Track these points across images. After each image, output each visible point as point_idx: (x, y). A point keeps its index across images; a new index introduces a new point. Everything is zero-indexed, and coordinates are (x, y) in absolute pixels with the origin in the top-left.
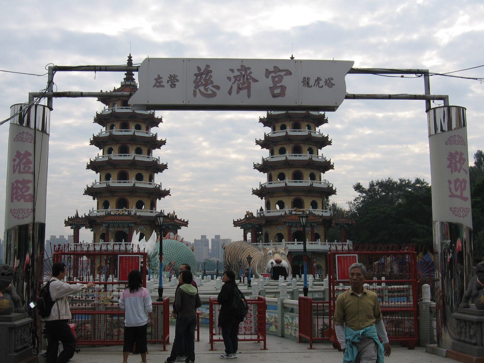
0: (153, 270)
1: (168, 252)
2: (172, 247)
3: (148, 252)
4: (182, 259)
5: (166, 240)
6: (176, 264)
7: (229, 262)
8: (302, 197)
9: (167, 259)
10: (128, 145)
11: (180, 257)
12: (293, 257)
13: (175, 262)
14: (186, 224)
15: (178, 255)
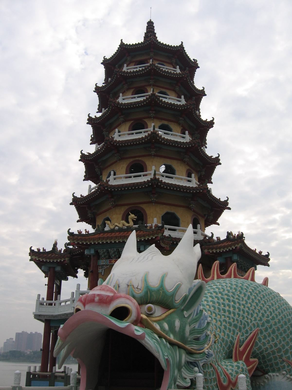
0: (190, 353)
1: (237, 305)
2: (245, 295)
3: (162, 281)
4: (274, 327)
5: (228, 279)
6: (260, 340)
9: (235, 326)
10: (146, 120)
11: (268, 322)
13: (256, 335)
14: (264, 260)
15: (263, 315)
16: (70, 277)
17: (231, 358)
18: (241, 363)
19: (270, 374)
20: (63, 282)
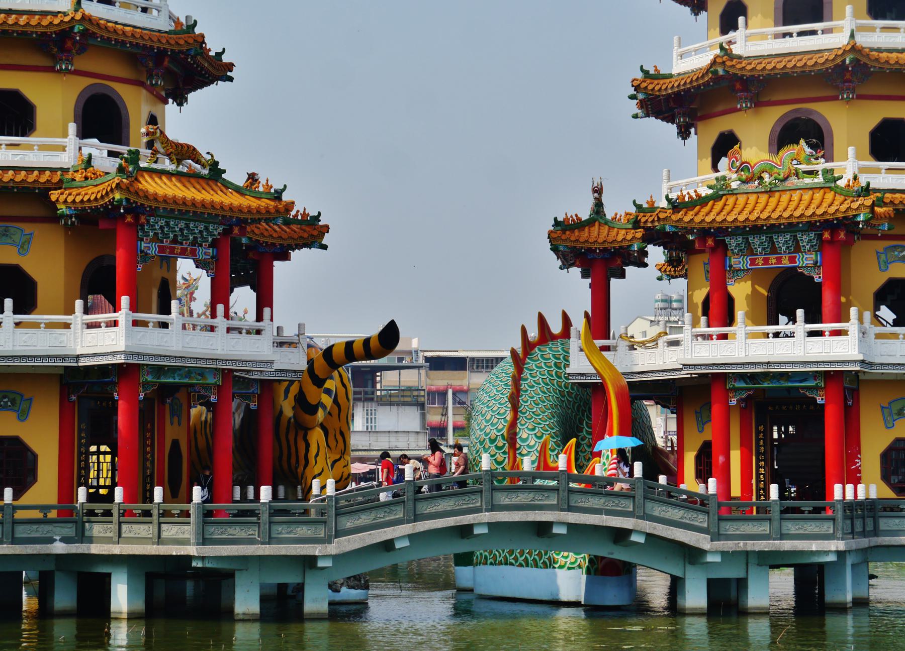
16: (630, 270)
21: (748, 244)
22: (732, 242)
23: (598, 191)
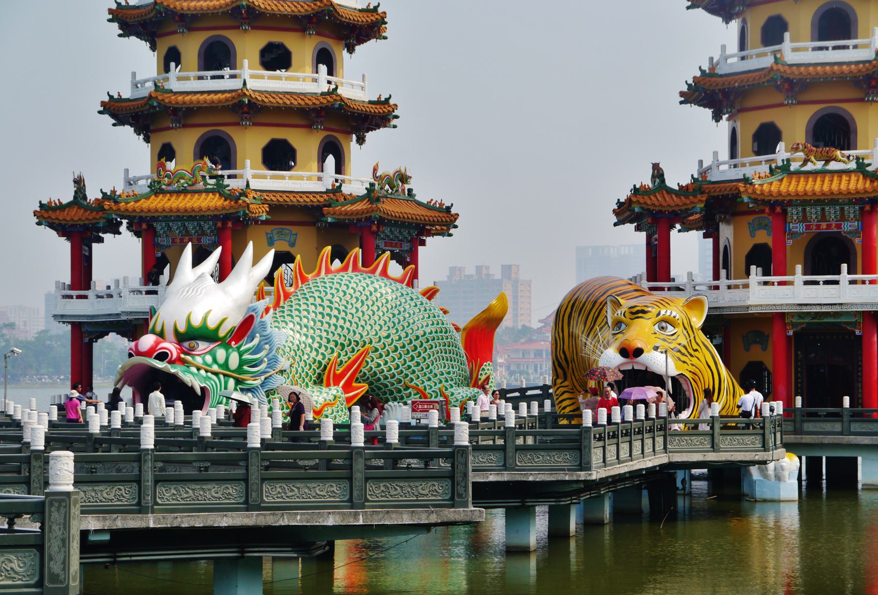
7: (564, 352)
8: (845, 106)
12: (791, 333)
16: (107, 237)
17: (321, 382)
18: (336, 391)
19: (390, 403)
20: (94, 245)
21: (170, 228)
22: (158, 226)
23: (79, 182)
